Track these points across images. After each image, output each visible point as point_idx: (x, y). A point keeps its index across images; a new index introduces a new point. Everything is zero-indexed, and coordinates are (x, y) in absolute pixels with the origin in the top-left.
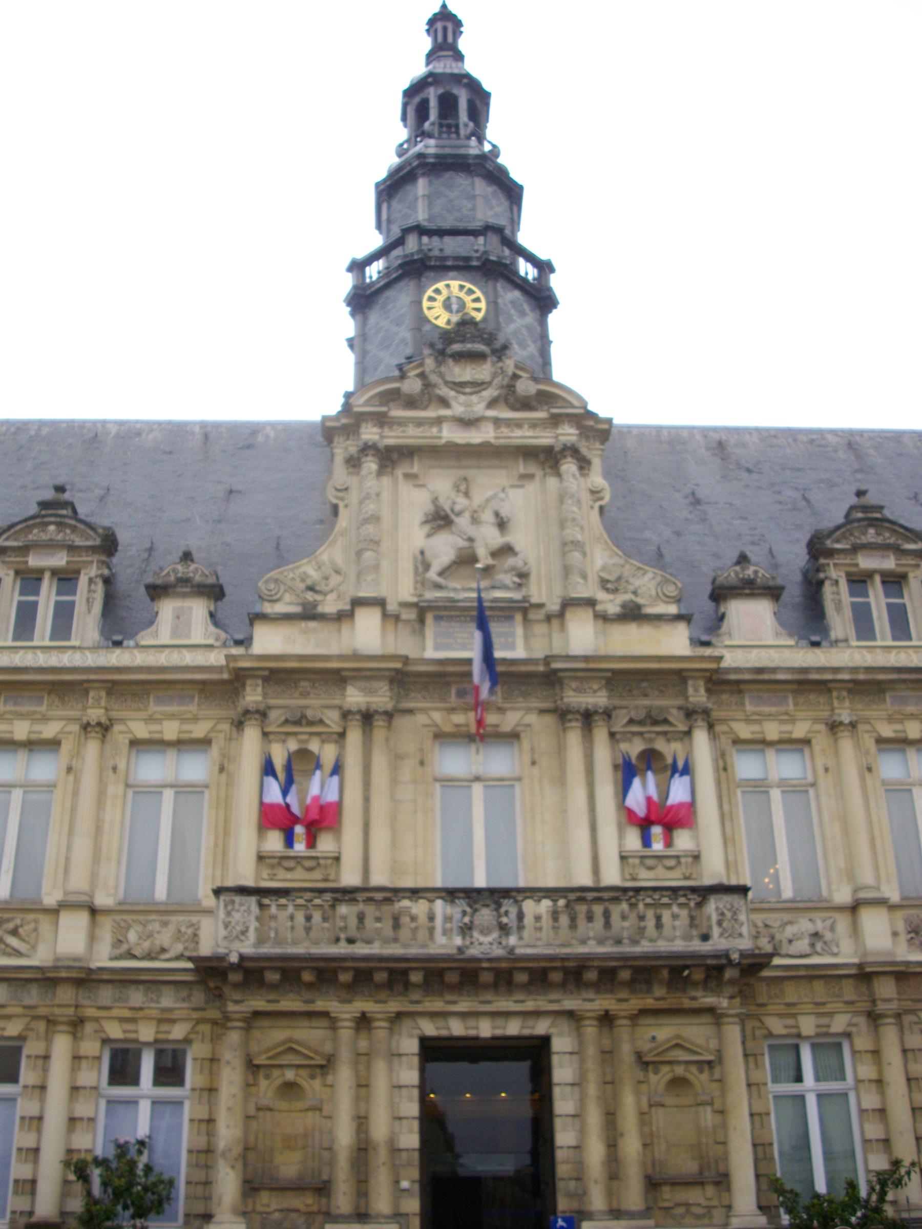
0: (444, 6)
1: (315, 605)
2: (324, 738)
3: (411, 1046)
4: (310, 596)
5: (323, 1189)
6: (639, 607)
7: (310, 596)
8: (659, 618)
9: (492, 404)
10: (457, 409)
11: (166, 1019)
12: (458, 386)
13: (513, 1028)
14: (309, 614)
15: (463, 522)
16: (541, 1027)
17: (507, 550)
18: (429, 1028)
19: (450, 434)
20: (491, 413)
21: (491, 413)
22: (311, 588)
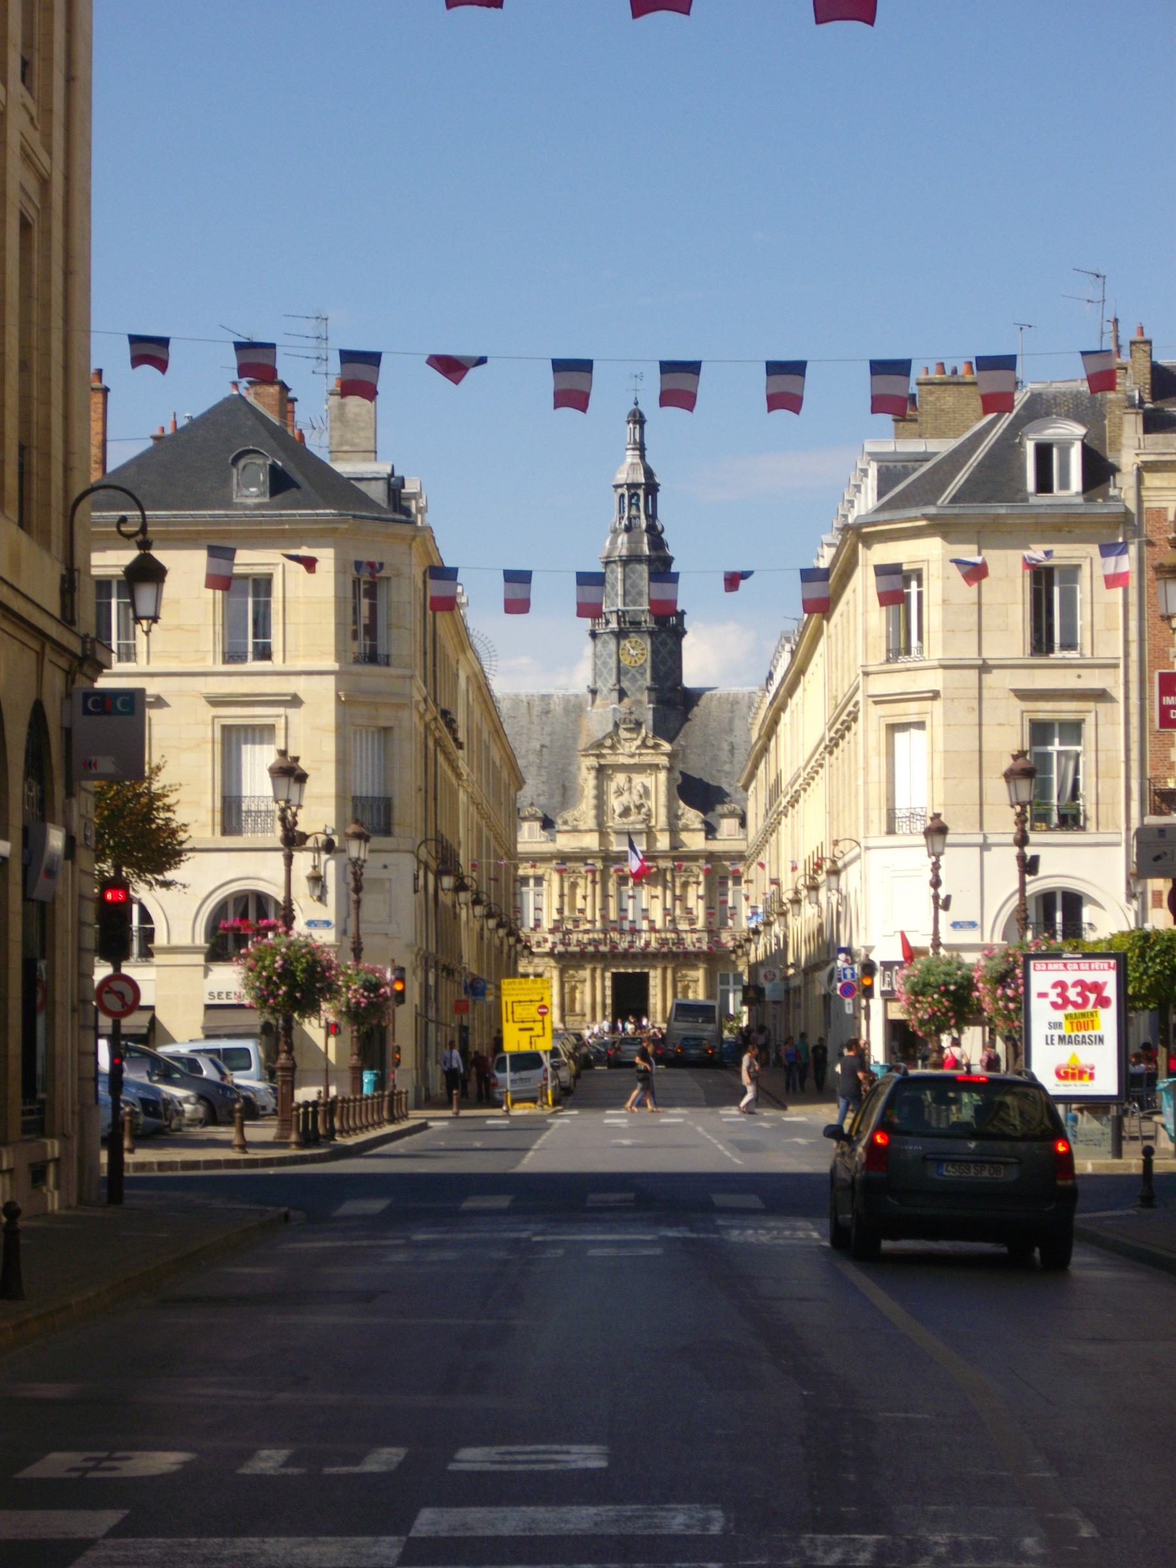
0: (636, 404)
1: (577, 826)
2: (582, 877)
3: (608, 975)
4: (575, 823)
5: (584, 1015)
6: (688, 825)
7: (575, 823)
8: (694, 830)
9: (638, 748)
10: (627, 751)
11: (537, 966)
12: (626, 740)
13: (638, 970)
14: (576, 830)
15: (626, 794)
16: (646, 970)
17: (642, 805)
18: (614, 970)
19: (623, 760)
20: (638, 751)
21: (638, 751)
22: (576, 820)
